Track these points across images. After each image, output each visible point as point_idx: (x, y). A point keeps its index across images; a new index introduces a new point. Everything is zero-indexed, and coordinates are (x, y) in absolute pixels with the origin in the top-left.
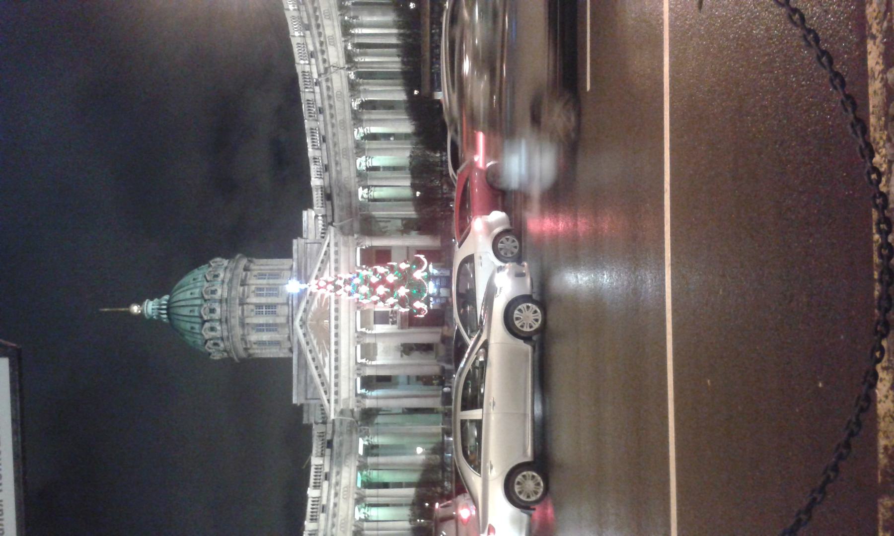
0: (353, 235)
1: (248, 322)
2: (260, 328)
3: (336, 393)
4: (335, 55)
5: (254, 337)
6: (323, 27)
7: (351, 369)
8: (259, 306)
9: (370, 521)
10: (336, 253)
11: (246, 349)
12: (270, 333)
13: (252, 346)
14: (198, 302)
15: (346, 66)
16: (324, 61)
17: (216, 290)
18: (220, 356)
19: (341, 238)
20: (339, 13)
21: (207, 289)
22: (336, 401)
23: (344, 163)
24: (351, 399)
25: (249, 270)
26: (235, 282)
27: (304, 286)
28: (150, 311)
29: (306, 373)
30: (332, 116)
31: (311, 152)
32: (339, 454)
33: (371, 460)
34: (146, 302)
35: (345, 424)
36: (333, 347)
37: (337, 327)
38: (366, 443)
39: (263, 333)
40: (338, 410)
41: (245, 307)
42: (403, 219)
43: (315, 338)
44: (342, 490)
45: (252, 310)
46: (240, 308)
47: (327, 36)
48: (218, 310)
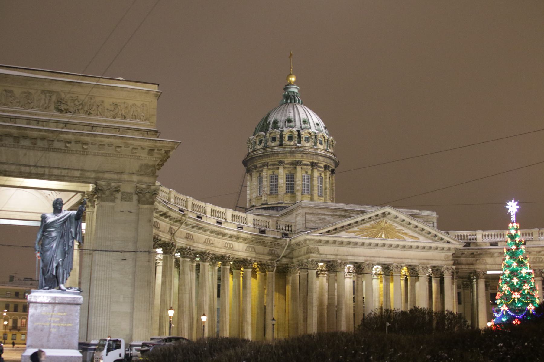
1: (298, 168)
2: (291, 179)
3: (327, 242)
5: (282, 172)
7: (345, 257)
8: (311, 178)
10: (443, 249)
13: (270, 169)
17: (322, 145)
19: (451, 254)
21: (323, 138)
22: (320, 241)
24: (318, 255)
26: (328, 160)
27: (513, 218)
29: (328, 215)
41: (310, 167)
43: (371, 225)
44: (231, 242)
45: (307, 173)
46: (309, 163)
48: (307, 145)
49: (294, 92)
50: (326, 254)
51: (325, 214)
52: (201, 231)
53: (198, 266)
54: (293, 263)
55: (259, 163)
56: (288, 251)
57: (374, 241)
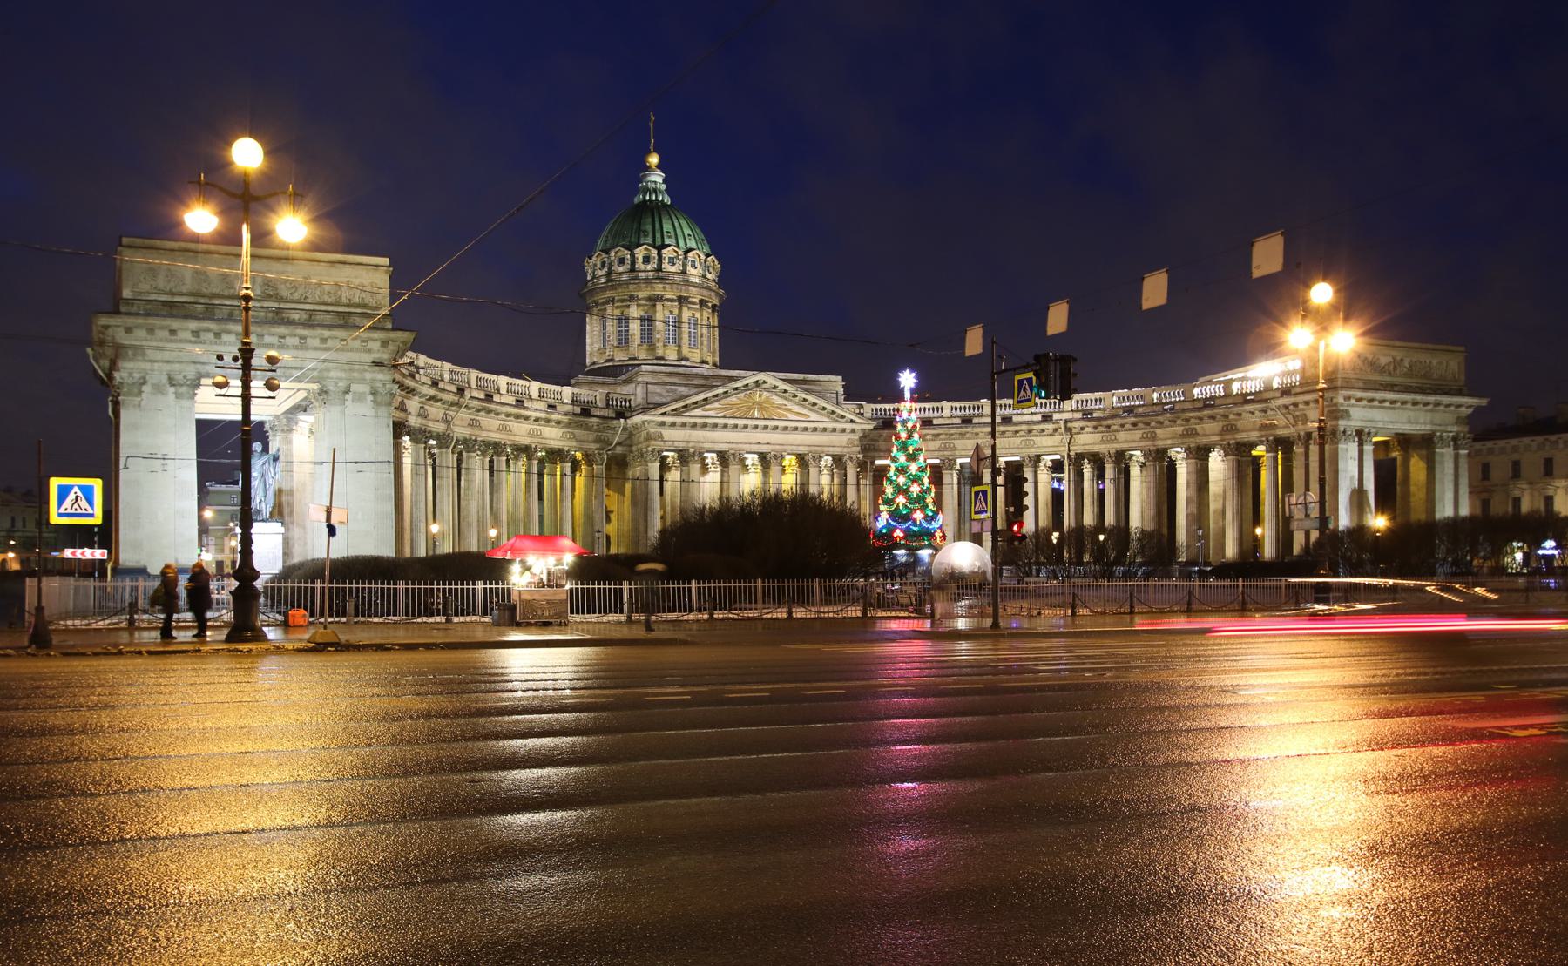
2: (648, 320)
3: (673, 424)
5: (634, 312)
7: (701, 445)
8: (678, 323)
10: (844, 430)
13: (617, 308)
14: (681, 243)
15: (1072, 453)
22: (663, 424)
23: (936, 444)
25: (713, 311)
26: (705, 292)
27: (907, 395)
29: (680, 385)
36: (731, 422)
37: (756, 427)
45: (671, 313)
48: (673, 269)
49: (655, 182)
51: (675, 384)
52: (492, 415)
53: (491, 461)
54: (632, 452)
55: (601, 297)
56: (625, 436)
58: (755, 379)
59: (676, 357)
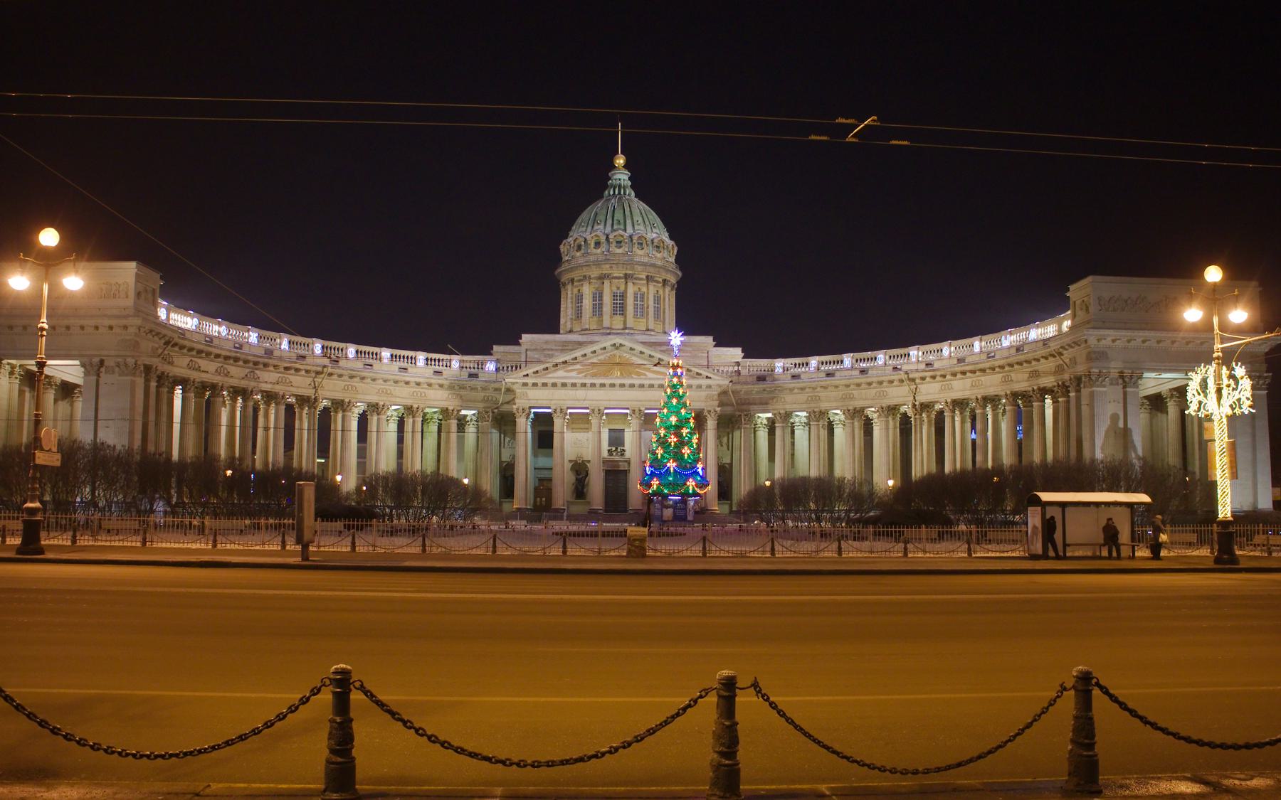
0: (718, 407)
2: (598, 297)
3: (535, 385)
4: (931, 392)
5: (587, 290)
6: (963, 379)
7: (562, 402)
8: (623, 296)
9: (422, 424)
10: (699, 387)
11: (572, 281)
12: (591, 308)
15: (917, 403)
16: (923, 379)
17: (643, 249)
18: (564, 252)
19: (716, 393)
20: (979, 397)
21: (643, 239)
22: (525, 384)
23: (803, 397)
24: (527, 401)
26: (652, 270)
28: (617, 176)
29: (556, 350)
30: (859, 385)
31: (814, 362)
32: (462, 387)
33: (454, 423)
34: (627, 172)
35: (495, 394)
37: (613, 385)
38: (468, 418)
39: (591, 300)
40: (514, 387)
42: (731, 464)
43: (599, 360)
45: (618, 288)
46: (622, 275)
47: (952, 382)
50: (537, 400)
51: (552, 350)
57: (607, 382)
58: (612, 342)
59: (621, 327)
